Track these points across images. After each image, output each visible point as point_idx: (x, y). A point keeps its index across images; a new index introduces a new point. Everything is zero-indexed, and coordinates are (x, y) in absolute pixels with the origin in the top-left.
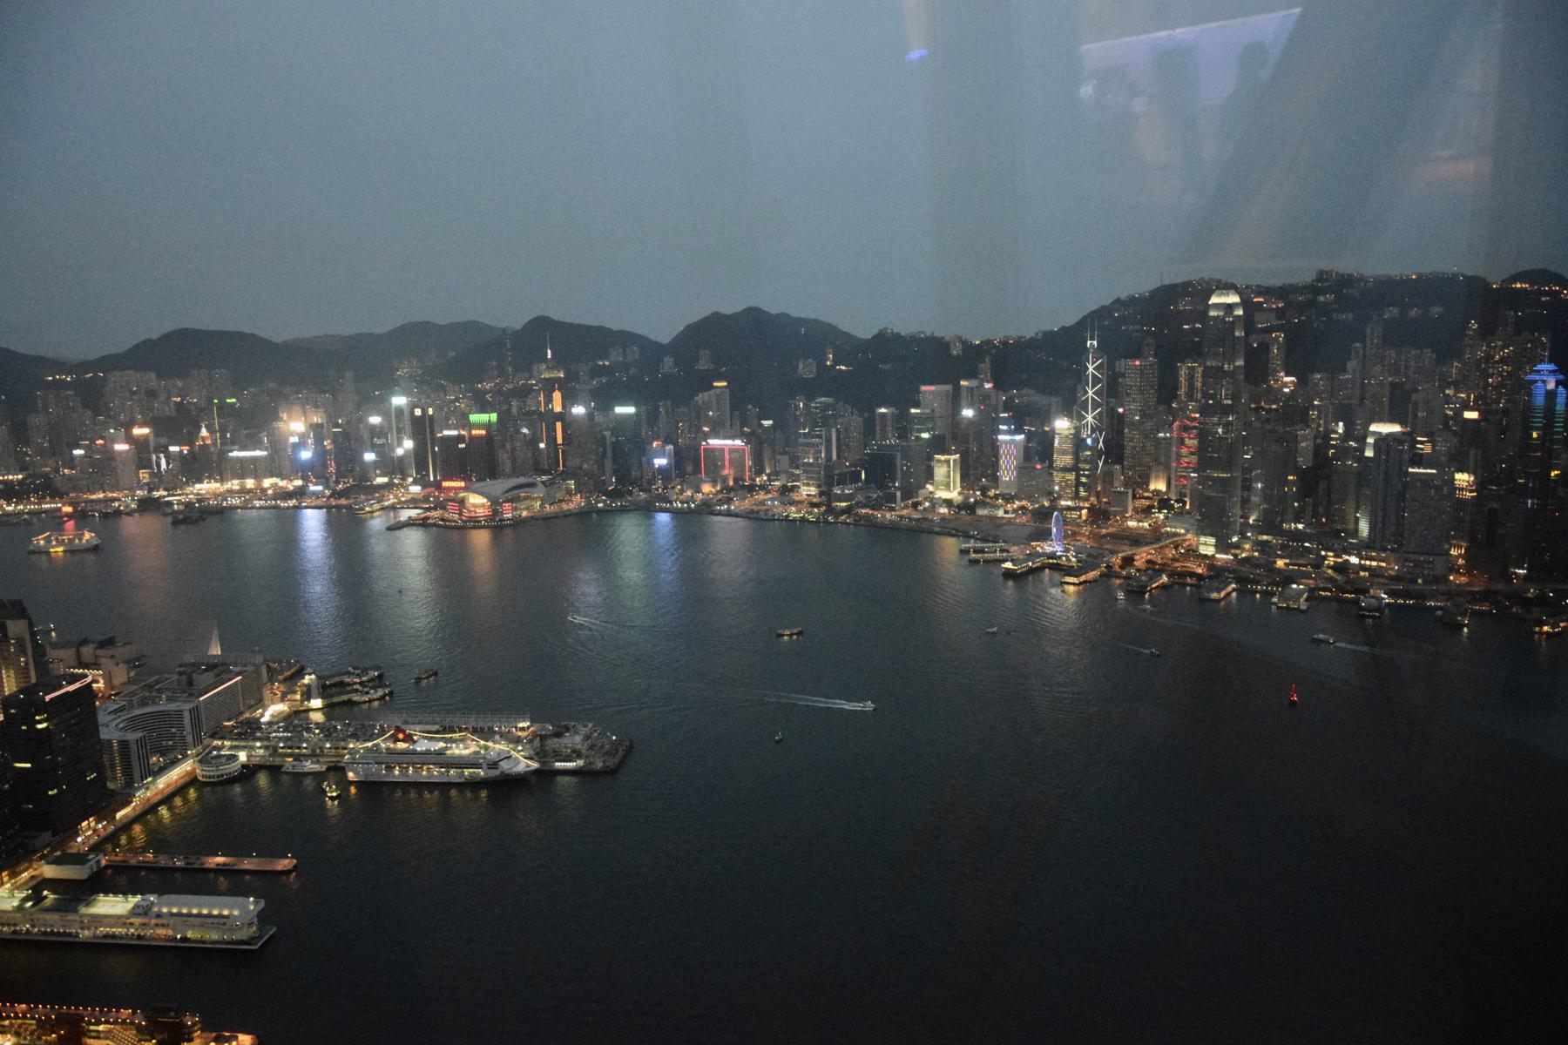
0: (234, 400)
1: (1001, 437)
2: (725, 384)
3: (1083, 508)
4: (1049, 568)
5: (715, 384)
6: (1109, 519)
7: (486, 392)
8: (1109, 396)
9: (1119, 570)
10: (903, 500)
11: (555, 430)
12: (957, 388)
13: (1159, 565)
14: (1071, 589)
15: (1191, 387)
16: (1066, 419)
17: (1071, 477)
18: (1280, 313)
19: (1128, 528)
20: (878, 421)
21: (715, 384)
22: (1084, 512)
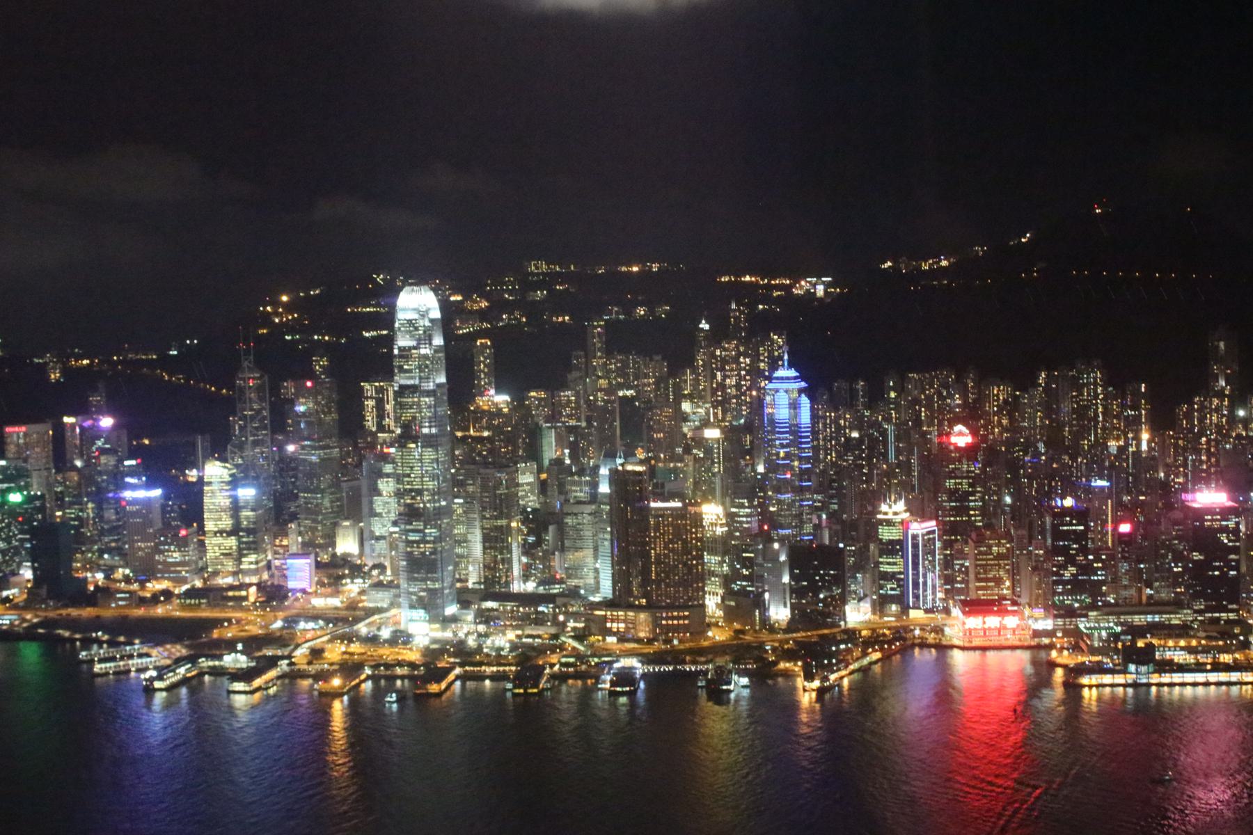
1: (128, 494)
4: (210, 674)
6: (286, 597)
8: (274, 432)
12: (60, 428)
13: (358, 654)
15: (381, 413)
16: (218, 463)
17: (232, 542)
18: (483, 315)
19: (314, 607)
22: (253, 590)
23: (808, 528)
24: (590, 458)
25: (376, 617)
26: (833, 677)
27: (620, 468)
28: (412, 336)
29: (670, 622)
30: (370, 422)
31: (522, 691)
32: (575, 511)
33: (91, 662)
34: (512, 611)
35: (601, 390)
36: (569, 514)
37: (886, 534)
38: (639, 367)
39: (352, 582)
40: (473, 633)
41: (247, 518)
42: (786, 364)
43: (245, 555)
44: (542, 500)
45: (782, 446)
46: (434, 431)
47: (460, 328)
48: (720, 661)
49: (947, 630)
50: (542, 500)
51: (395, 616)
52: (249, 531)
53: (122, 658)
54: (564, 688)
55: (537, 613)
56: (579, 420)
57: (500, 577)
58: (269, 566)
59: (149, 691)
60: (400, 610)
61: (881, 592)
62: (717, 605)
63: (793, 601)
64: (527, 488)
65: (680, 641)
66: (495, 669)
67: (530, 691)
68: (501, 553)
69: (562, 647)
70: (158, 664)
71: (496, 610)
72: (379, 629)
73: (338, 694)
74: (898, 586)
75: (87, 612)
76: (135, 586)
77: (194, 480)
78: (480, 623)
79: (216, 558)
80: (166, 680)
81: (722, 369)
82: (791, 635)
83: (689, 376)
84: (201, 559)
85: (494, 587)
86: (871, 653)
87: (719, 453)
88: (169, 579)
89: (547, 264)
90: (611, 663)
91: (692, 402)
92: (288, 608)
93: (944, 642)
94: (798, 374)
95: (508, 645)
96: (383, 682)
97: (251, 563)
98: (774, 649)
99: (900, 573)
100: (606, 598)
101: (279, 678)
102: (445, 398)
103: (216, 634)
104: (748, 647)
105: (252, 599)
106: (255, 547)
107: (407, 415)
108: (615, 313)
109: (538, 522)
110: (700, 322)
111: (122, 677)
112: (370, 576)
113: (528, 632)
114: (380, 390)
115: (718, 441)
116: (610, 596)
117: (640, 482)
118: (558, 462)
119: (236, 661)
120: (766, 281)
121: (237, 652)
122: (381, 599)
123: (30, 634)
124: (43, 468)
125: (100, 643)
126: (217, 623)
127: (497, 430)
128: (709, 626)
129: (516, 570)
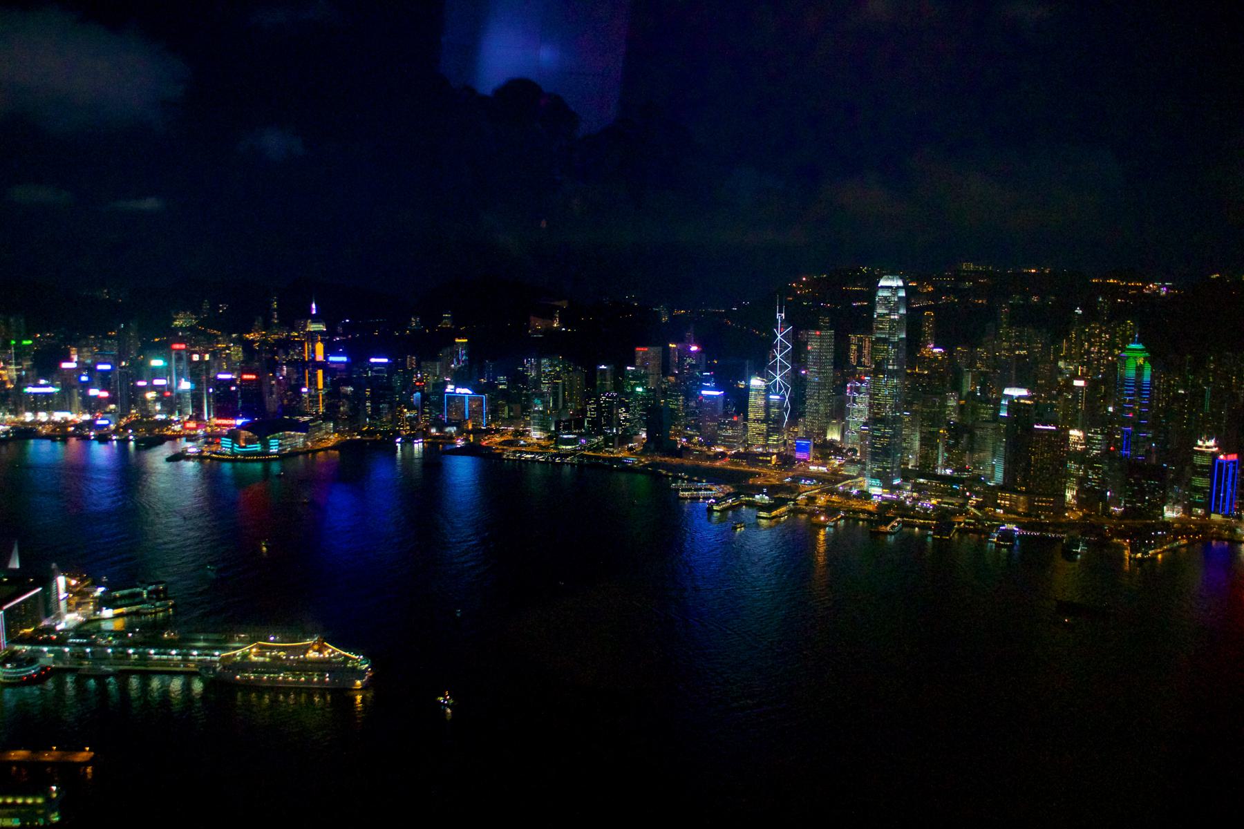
0: (30, 342)
2: (466, 340)
3: (773, 454)
4: (746, 505)
5: (457, 340)
7: (253, 341)
9: (804, 507)
10: (619, 446)
11: (316, 376)
12: (667, 350)
13: (837, 503)
14: (764, 522)
15: (859, 357)
16: (759, 378)
17: (764, 426)
20: (598, 374)
21: (457, 340)
22: (774, 457)
23: (1142, 451)
24: (993, 393)
25: (849, 481)
26: (1150, 552)
27: (1016, 401)
28: (887, 308)
29: (1040, 504)
30: (853, 361)
31: (939, 537)
32: (982, 426)
33: (677, 490)
34: (936, 486)
35: (1004, 349)
36: (977, 428)
37: (1198, 460)
38: (1031, 336)
39: (835, 458)
40: (909, 498)
41: (774, 413)
42: (1136, 340)
43: (771, 436)
44: (960, 417)
45: (1129, 395)
46: (895, 367)
47: (914, 304)
48: (1073, 533)
49: (1239, 530)
50: (960, 417)
51: (861, 482)
52: (775, 421)
53: (695, 490)
54: (965, 537)
55: (952, 489)
56: (988, 367)
57: (930, 464)
58: (785, 443)
59: (710, 510)
60: (865, 478)
61: (1191, 499)
62: (1073, 495)
63: (1127, 499)
64: (951, 409)
65: (1046, 517)
66: (922, 521)
67: (944, 537)
68: (932, 449)
69: (967, 512)
70: (716, 495)
71: (926, 484)
72: (851, 489)
73: (823, 526)
74: (1205, 497)
75: (676, 461)
76: (705, 448)
77: (743, 387)
78: (913, 492)
79: (754, 435)
80: (720, 506)
81: (1089, 341)
82: (1121, 522)
83: (1065, 345)
84: (744, 435)
85: (927, 468)
86: (1179, 539)
87: (1082, 397)
88: (724, 446)
89: (974, 265)
90: (999, 526)
91: (1066, 361)
92: (794, 470)
93: (1236, 539)
94: (1144, 347)
95: (931, 507)
96: (851, 521)
97: (774, 440)
98: (1111, 530)
99: (1207, 488)
100: (997, 484)
101: (788, 511)
102: (904, 348)
103: (751, 481)
104: (1092, 525)
105: (773, 463)
106: (777, 430)
107: (879, 358)
108: (1016, 299)
109: (957, 431)
110: (1076, 309)
111: (694, 501)
112: (847, 456)
113: (944, 500)
114: (860, 340)
115: (1081, 388)
116: (1002, 483)
117: (1028, 411)
118: (973, 393)
119: (762, 499)
120: (1124, 283)
121: (763, 494)
122: (852, 470)
123: (643, 470)
124: (655, 373)
125: (683, 479)
126: (753, 474)
127: (933, 371)
128: (1066, 509)
129: (940, 462)
